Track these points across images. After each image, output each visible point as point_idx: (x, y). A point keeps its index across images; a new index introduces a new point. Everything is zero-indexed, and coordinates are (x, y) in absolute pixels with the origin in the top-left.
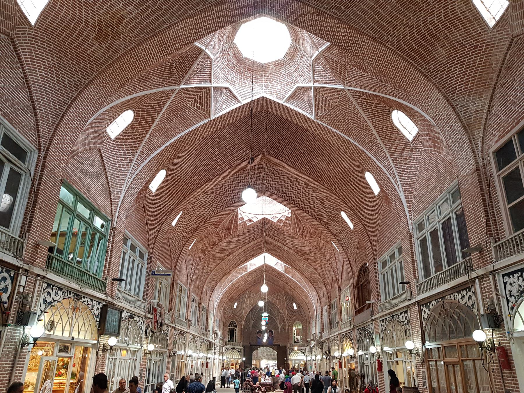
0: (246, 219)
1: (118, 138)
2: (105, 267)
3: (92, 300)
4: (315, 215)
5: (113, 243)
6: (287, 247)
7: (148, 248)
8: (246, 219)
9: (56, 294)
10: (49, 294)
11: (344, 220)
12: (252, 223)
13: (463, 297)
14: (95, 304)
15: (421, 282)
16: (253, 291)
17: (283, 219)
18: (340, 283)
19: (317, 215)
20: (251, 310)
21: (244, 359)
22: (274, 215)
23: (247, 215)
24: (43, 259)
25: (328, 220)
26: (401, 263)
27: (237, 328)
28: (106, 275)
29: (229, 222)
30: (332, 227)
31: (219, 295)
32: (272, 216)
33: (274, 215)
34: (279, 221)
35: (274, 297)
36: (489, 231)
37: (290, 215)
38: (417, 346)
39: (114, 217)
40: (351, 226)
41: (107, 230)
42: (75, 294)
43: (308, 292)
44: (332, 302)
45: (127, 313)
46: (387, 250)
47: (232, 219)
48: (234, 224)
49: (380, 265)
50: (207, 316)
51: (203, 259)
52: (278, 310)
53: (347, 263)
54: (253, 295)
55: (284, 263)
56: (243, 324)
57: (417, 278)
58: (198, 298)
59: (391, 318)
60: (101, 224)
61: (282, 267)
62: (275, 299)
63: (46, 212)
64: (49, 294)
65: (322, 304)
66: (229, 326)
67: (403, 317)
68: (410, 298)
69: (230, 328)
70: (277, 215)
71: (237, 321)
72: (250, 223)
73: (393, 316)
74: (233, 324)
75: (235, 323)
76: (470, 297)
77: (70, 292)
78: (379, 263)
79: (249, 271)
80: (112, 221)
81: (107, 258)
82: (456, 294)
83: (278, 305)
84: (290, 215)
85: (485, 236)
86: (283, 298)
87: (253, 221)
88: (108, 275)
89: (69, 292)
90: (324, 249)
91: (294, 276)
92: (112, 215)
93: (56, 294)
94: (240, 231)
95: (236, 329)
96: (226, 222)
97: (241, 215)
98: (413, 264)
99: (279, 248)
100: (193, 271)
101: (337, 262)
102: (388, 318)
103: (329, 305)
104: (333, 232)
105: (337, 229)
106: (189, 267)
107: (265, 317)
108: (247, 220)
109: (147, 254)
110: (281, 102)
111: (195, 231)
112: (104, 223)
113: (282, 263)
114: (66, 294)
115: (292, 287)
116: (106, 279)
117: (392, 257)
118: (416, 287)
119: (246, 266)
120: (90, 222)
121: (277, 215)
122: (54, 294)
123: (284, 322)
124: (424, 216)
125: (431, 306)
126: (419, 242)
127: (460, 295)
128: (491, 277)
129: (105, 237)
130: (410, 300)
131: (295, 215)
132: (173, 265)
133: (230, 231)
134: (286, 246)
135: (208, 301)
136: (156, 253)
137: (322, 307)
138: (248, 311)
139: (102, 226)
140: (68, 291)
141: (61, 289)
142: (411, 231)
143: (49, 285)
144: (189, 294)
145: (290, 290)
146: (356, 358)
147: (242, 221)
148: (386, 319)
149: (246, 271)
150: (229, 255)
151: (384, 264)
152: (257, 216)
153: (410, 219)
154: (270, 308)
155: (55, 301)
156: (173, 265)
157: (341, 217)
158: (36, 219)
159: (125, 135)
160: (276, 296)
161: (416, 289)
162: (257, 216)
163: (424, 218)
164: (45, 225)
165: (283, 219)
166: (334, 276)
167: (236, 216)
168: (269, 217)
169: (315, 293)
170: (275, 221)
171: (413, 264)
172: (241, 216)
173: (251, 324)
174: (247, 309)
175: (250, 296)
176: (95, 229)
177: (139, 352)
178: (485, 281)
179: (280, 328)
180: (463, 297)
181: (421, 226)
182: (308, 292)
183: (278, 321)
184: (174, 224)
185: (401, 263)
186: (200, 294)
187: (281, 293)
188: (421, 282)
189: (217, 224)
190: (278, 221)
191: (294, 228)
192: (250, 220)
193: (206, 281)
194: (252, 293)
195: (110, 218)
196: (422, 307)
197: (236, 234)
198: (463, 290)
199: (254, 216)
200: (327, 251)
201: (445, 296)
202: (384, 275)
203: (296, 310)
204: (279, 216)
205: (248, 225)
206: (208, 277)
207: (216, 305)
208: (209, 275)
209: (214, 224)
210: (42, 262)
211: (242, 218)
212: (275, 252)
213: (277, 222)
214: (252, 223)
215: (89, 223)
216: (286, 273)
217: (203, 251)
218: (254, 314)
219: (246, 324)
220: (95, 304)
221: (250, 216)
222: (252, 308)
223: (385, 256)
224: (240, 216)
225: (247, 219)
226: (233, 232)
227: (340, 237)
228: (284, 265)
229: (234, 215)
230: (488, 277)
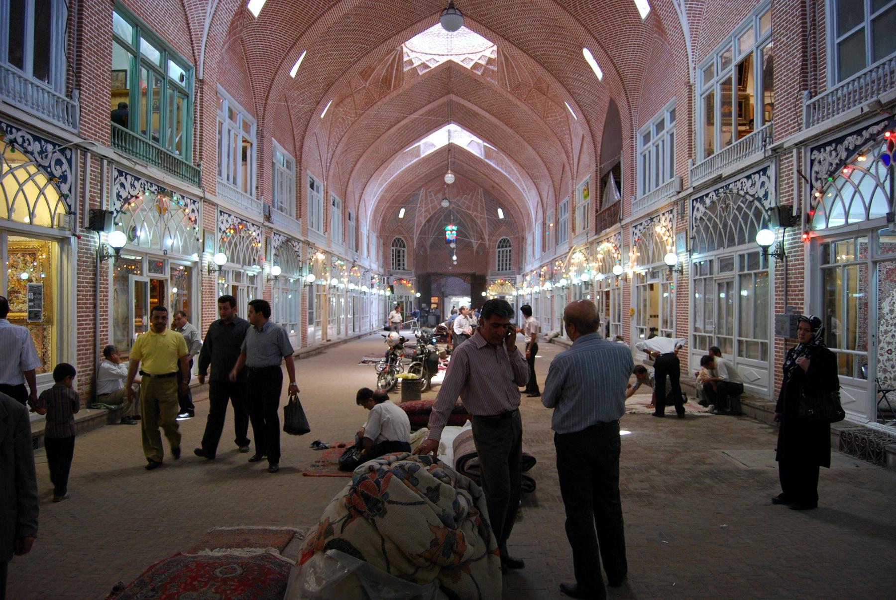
0: (417, 63)
2: (195, 146)
3: (183, 197)
4: (538, 55)
5: (201, 105)
6: (489, 112)
7: (256, 115)
8: (417, 63)
9: (133, 185)
10: (122, 185)
11: (587, 63)
12: (427, 70)
13: (753, 185)
14: (189, 203)
15: (698, 163)
17: (483, 62)
18: (575, 172)
19: (542, 55)
20: (429, 221)
21: (418, 295)
22: (467, 56)
23: (418, 55)
24: (106, 132)
25: (560, 63)
26: (672, 135)
27: (405, 249)
28: (198, 159)
29: (387, 70)
30: (567, 77)
31: (374, 196)
32: (463, 57)
33: (467, 56)
34: (476, 66)
35: (466, 199)
36: (803, 81)
37: (494, 56)
38: (680, 260)
39: (198, 63)
40: (599, 74)
41: (189, 84)
42: (158, 187)
43: (524, 189)
44: (561, 204)
45: (235, 219)
46: (653, 115)
47: (392, 65)
48: (396, 73)
49: (639, 139)
50: (357, 229)
51: (346, 135)
52: (473, 220)
53: (588, 139)
54: (431, 196)
55: (484, 141)
56: (415, 242)
57: (693, 158)
58: (341, 201)
59: (649, 221)
60: (179, 74)
61: (480, 149)
62: (467, 202)
63: (98, 55)
64: (122, 185)
65: (545, 205)
66: (393, 246)
68: (678, 190)
69: (394, 248)
70: (470, 56)
71: (405, 237)
72: (425, 71)
73: (652, 219)
74: (399, 243)
75: (402, 241)
76: (763, 184)
77: (151, 184)
78: (638, 135)
79: (422, 156)
80: (196, 68)
81: (195, 131)
82: (745, 180)
84: (494, 56)
85: (796, 89)
86: (481, 200)
87: (429, 67)
88: (201, 158)
89: (149, 184)
90: (552, 116)
91: (500, 163)
92: (195, 59)
93: (133, 185)
94: (406, 85)
95: (404, 251)
96: (381, 71)
97: (408, 56)
98: (690, 136)
99: (476, 115)
100: (330, 155)
101: (573, 137)
102: (644, 223)
103: (556, 209)
104: (567, 85)
105: (576, 79)
106: (323, 147)
108: (419, 66)
109: (255, 125)
111: (329, 85)
112: (184, 73)
113: (480, 141)
114: (146, 187)
115: (497, 181)
116: (199, 165)
117: (660, 126)
118: (689, 172)
119: (419, 147)
120: (163, 72)
122: (130, 186)
124: (715, 56)
125: (708, 201)
126: (702, 100)
127: (750, 181)
128: (795, 151)
129: (188, 97)
130: (679, 193)
131: (504, 55)
132: (297, 144)
133: (390, 85)
134: (486, 110)
135: (357, 204)
136: (269, 123)
137: (544, 212)
138: (424, 222)
139: (182, 78)
140: (147, 182)
141: (138, 179)
142: (692, 81)
143: (121, 173)
144: (327, 192)
145: (493, 187)
146: (592, 285)
147: (410, 68)
148: (641, 224)
149: (419, 156)
150: (389, 128)
151: (647, 138)
152: (436, 58)
153: (693, 61)
154: (459, 217)
155: (132, 196)
156: (297, 144)
157: (583, 58)
158: (86, 68)
160: (469, 197)
161: (689, 175)
162: (436, 58)
163: (715, 60)
164: (100, 77)
165: (483, 62)
166: (566, 160)
167: (399, 58)
168: (457, 60)
169: (534, 192)
170: (469, 66)
171: (690, 136)
173: (429, 243)
174: (420, 219)
175: (426, 199)
176: (172, 83)
177: (259, 278)
178: (786, 159)
179: (475, 249)
180: (753, 185)
181: (708, 74)
182: (524, 189)
184: (293, 73)
185: (672, 135)
186: (344, 194)
187: (478, 192)
188: (698, 163)
189: (366, 73)
191: (501, 79)
192: (424, 66)
193: (351, 172)
194: (430, 192)
195: (191, 64)
196: (695, 202)
197: (400, 91)
198: (754, 173)
199: (429, 57)
200: (557, 119)
201: (729, 185)
202: (645, 156)
203: (502, 219)
204: (476, 58)
205: (420, 74)
206: (355, 165)
207: (370, 212)
208: (357, 162)
209: (361, 73)
210: (105, 136)
211: (410, 62)
212: (469, 123)
213: (471, 68)
214: (427, 70)
215: (160, 74)
217: (344, 121)
218: (433, 227)
219: (421, 244)
220: (189, 203)
221: (425, 59)
222: (429, 216)
223: (650, 125)
224: (406, 59)
226: (394, 85)
227: (579, 94)
228: (485, 147)
229: (395, 57)
230: (792, 152)
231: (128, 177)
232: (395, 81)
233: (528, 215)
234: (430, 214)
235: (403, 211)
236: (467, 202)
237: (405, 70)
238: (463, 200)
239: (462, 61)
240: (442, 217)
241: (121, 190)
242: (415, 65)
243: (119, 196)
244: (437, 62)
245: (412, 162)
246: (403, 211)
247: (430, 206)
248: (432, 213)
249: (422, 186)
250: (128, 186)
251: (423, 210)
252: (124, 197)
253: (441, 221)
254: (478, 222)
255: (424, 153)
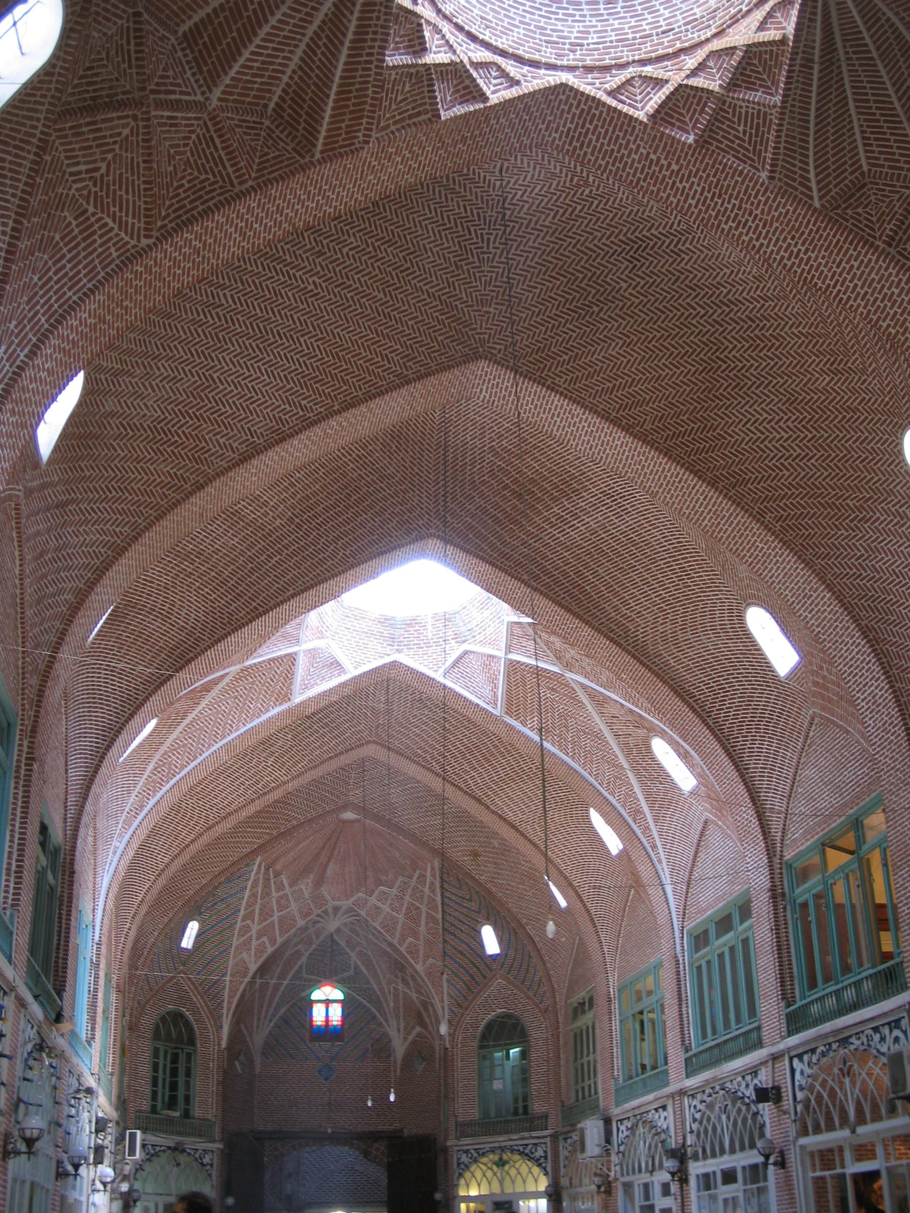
16: (278, 867)
35: (383, 897)
61: (493, 681)
65: (776, 828)
72: (460, 110)
79: (298, 699)
83: (402, 939)
107: (327, 1002)
115: (510, 816)
119: (291, 659)
123: (422, 1023)
133: (312, 132)
138: (253, 967)
149: (287, 698)
150: (245, 459)
160: (394, 891)
165: (712, 83)
175: (267, 894)
183: (393, 1023)
190: (664, 113)
194: (277, 874)
203: (494, 957)
205: (444, 115)
213: (653, 117)
216: (509, 712)
222: (270, 950)
232: (337, 117)
234: (273, 941)
236: (386, 908)
238: (373, 900)
239: (611, 93)
240: (304, 959)
244: (514, 82)
245: (264, 717)
247: (275, 918)
248: (279, 941)
249: (260, 849)
251: (255, 928)
253: (299, 972)
254: (419, 967)
255: (306, 687)
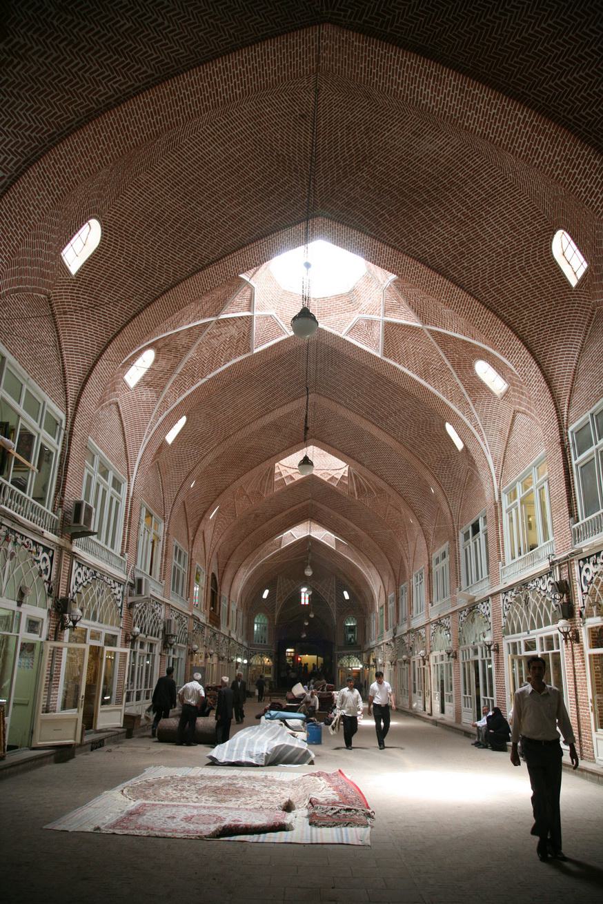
1: (138, 385)
32: (322, 472)
67: (484, 607)
72: (291, 482)
110: (341, 335)
113: (333, 536)
121: (329, 472)
147: (279, 478)
159: (146, 382)
170: (326, 479)
172: (278, 471)
190: (330, 479)
205: (287, 484)
211: (280, 474)
224: (276, 471)
225: (288, 474)
231: (84, 567)
233: (372, 597)
235: (267, 592)
237: (276, 480)
241: (78, 578)
242: (283, 476)
243: (77, 582)
246: (267, 592)
250: (82, 574)
252: (80, 583)
